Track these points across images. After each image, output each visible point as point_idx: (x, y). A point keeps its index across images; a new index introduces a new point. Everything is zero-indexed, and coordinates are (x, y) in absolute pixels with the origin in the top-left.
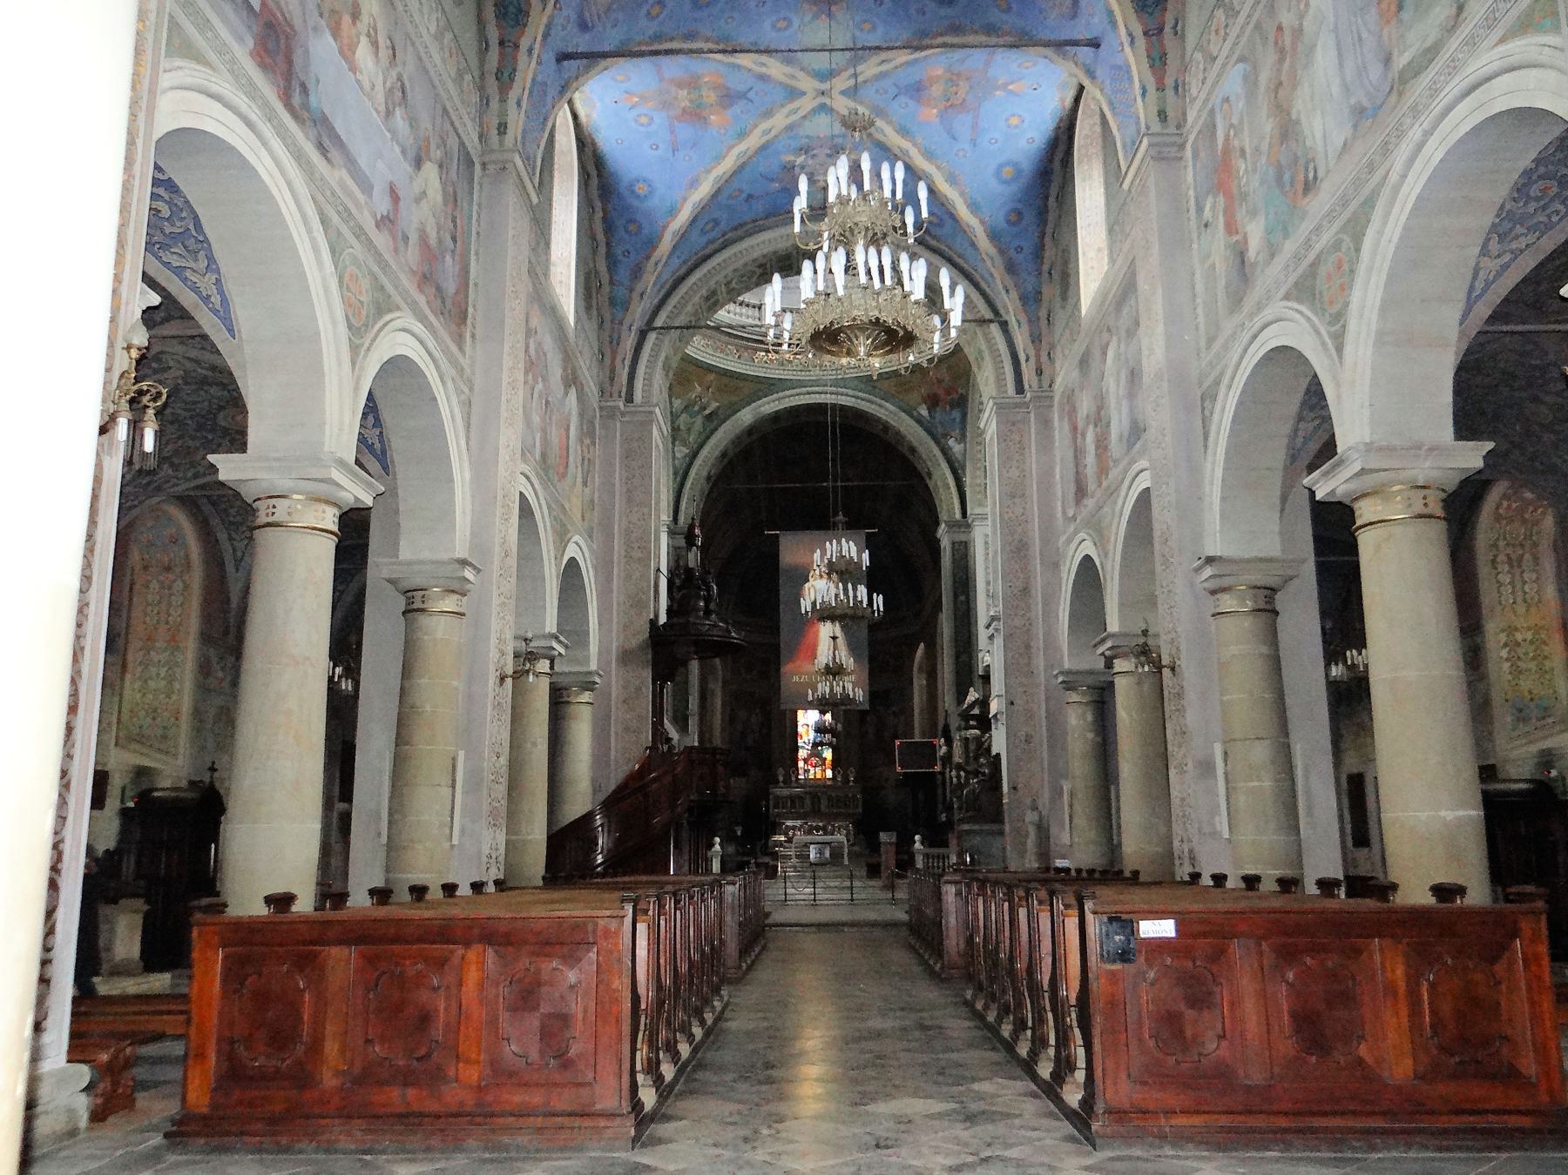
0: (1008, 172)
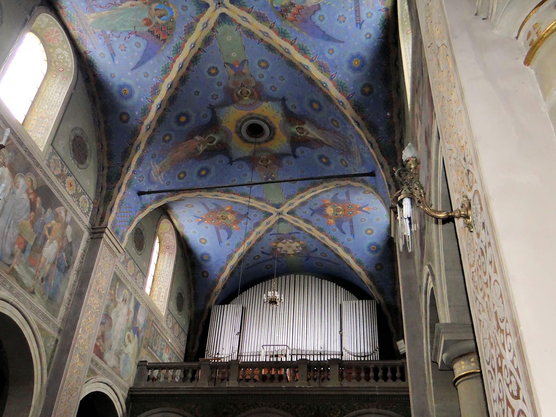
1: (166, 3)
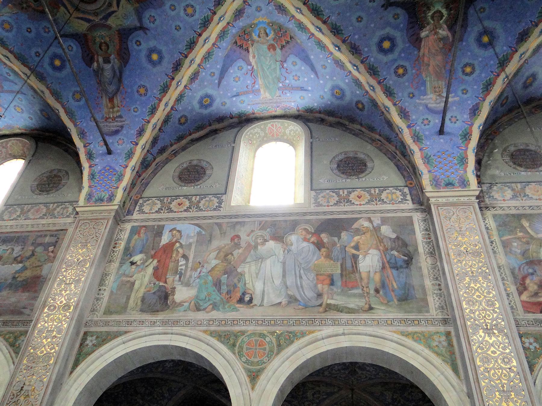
1: (253, 26)
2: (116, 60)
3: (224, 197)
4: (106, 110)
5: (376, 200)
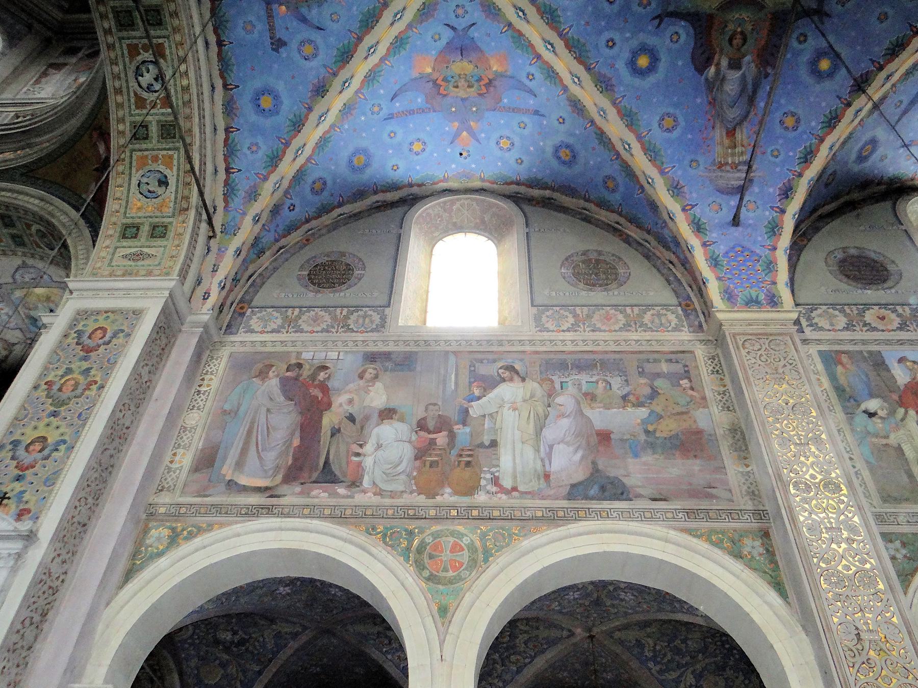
0: (358, 161)
2: (753, 65)
3: (387, 310)
4: (719, 149)
5: (636, 324)
